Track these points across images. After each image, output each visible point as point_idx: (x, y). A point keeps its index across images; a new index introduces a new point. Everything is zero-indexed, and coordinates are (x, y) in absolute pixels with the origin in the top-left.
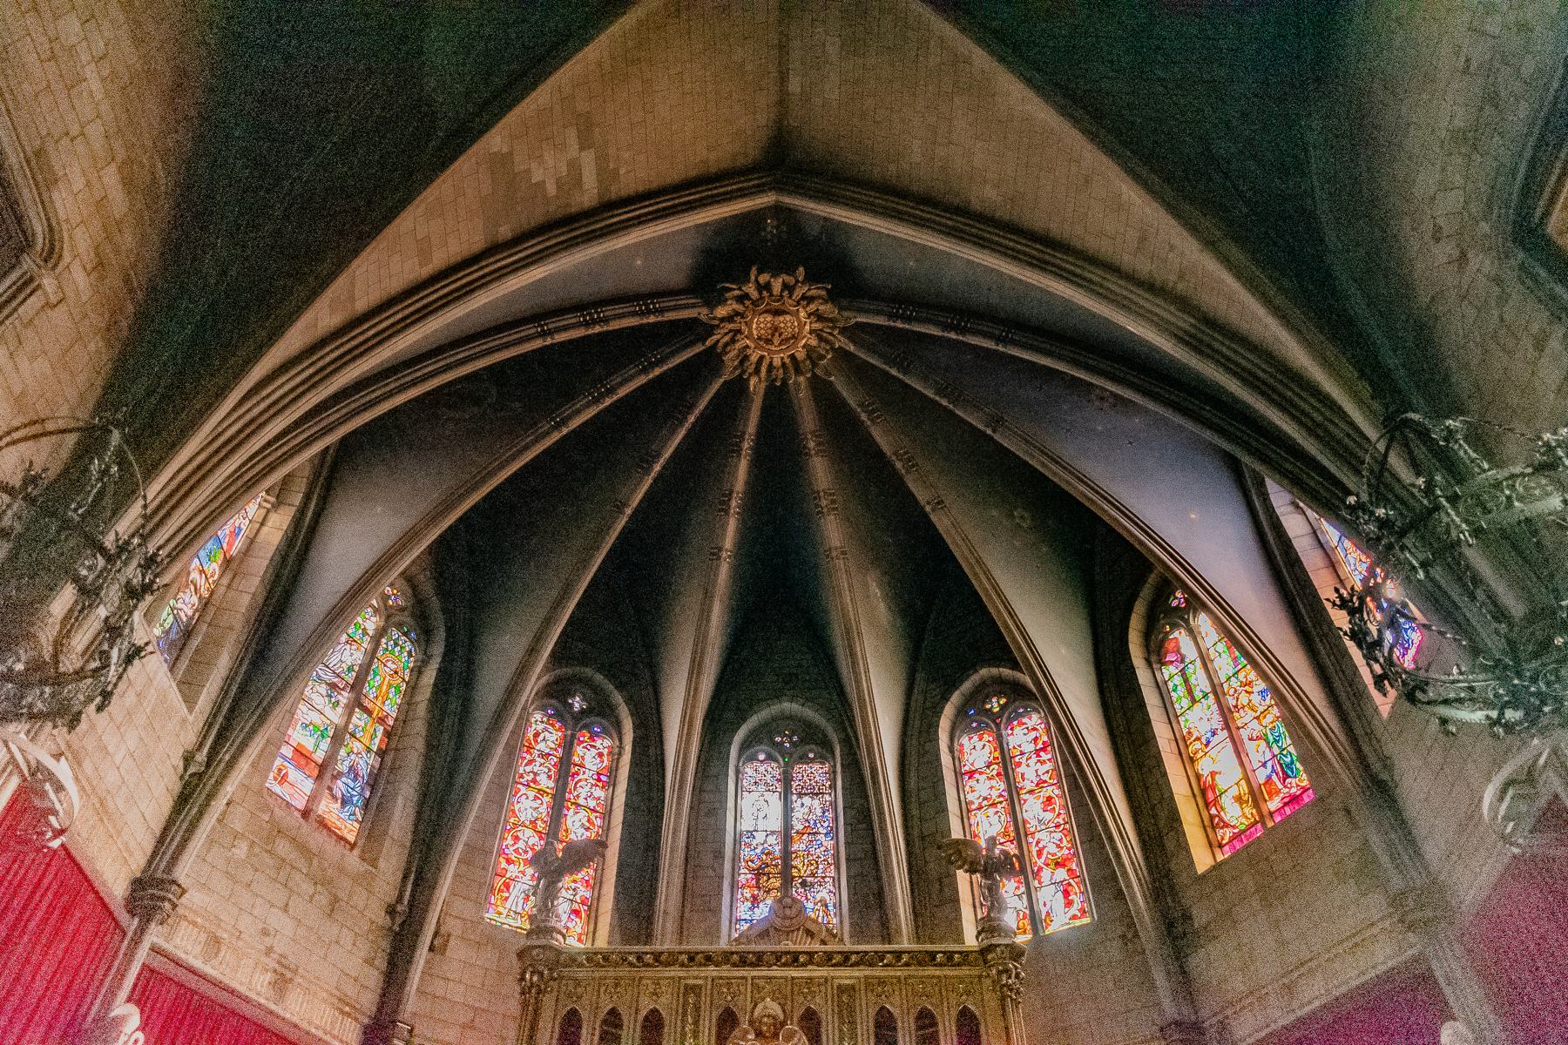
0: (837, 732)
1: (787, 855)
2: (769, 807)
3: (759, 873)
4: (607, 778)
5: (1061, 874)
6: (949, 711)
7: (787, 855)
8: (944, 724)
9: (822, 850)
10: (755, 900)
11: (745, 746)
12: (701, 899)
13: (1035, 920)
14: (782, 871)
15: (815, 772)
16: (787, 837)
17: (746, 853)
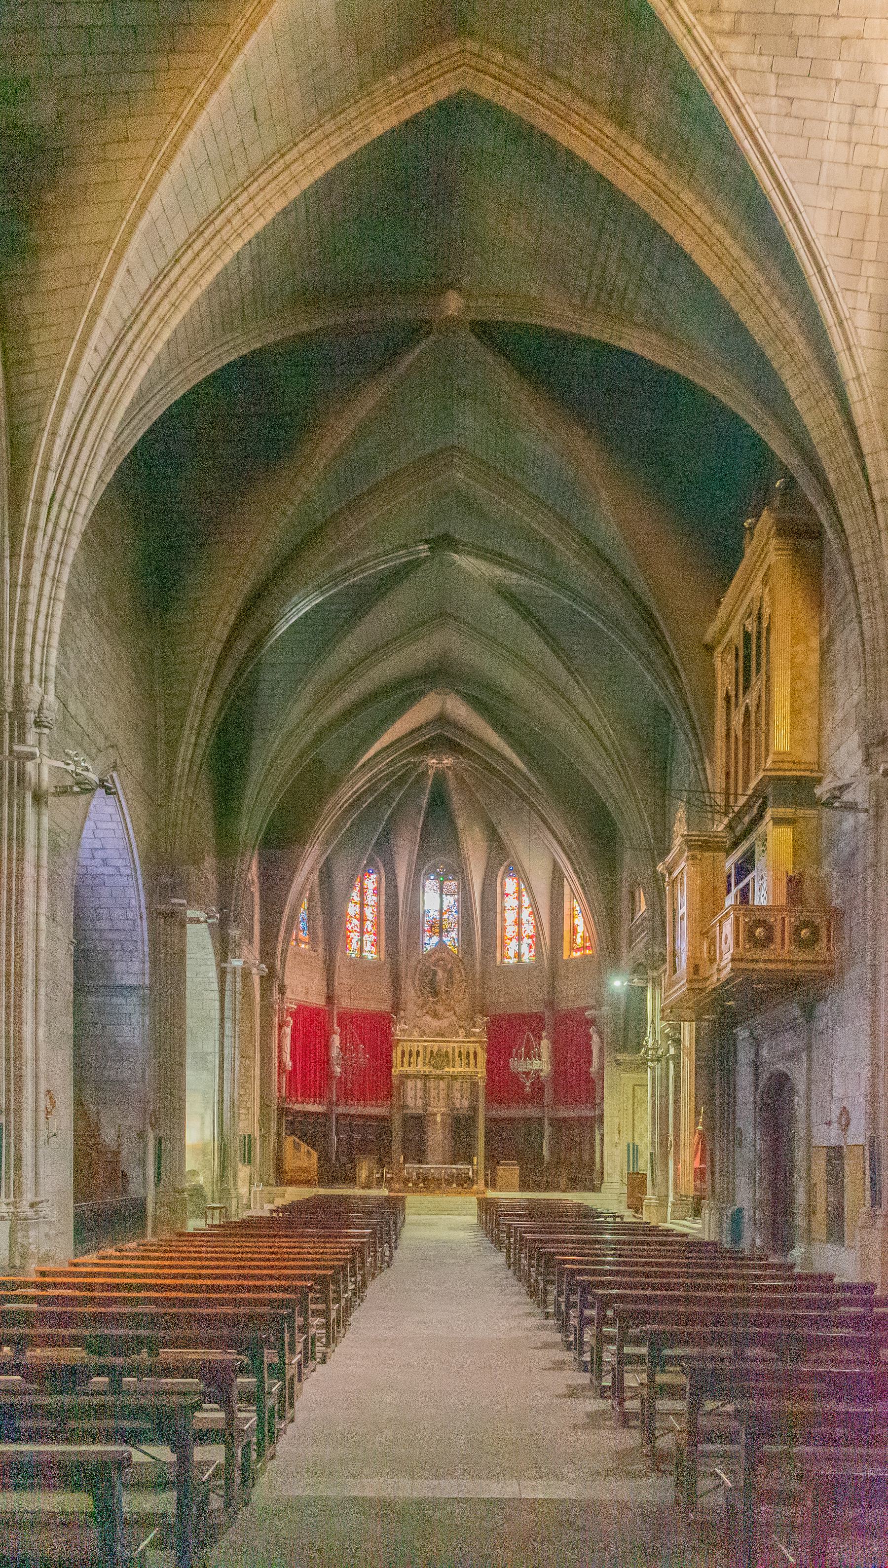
0: (459, 871)
1: (441, 919)
2: (434, 900)
3: (431, 926)
4: (377, 892)
5: (530, 941)
6: (502, 869)
7: (441, 919)
8: (500, 874)
9: (452, 918)
10: (431, 937)
11: (427, 873)
12: (414, 938)
13: (519, 955)
14: (439, 928)
15: (452, 885)
16: (441, 914)
17: (427, 918)
